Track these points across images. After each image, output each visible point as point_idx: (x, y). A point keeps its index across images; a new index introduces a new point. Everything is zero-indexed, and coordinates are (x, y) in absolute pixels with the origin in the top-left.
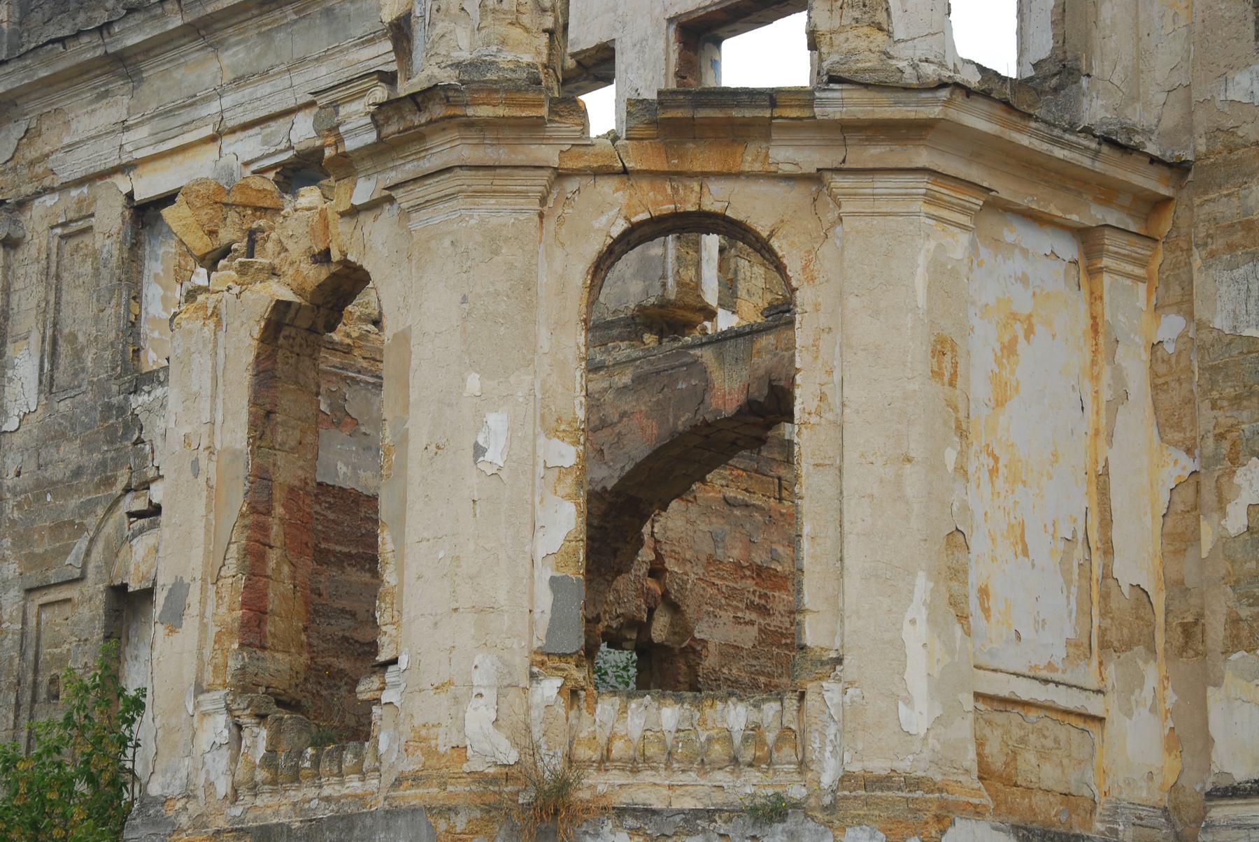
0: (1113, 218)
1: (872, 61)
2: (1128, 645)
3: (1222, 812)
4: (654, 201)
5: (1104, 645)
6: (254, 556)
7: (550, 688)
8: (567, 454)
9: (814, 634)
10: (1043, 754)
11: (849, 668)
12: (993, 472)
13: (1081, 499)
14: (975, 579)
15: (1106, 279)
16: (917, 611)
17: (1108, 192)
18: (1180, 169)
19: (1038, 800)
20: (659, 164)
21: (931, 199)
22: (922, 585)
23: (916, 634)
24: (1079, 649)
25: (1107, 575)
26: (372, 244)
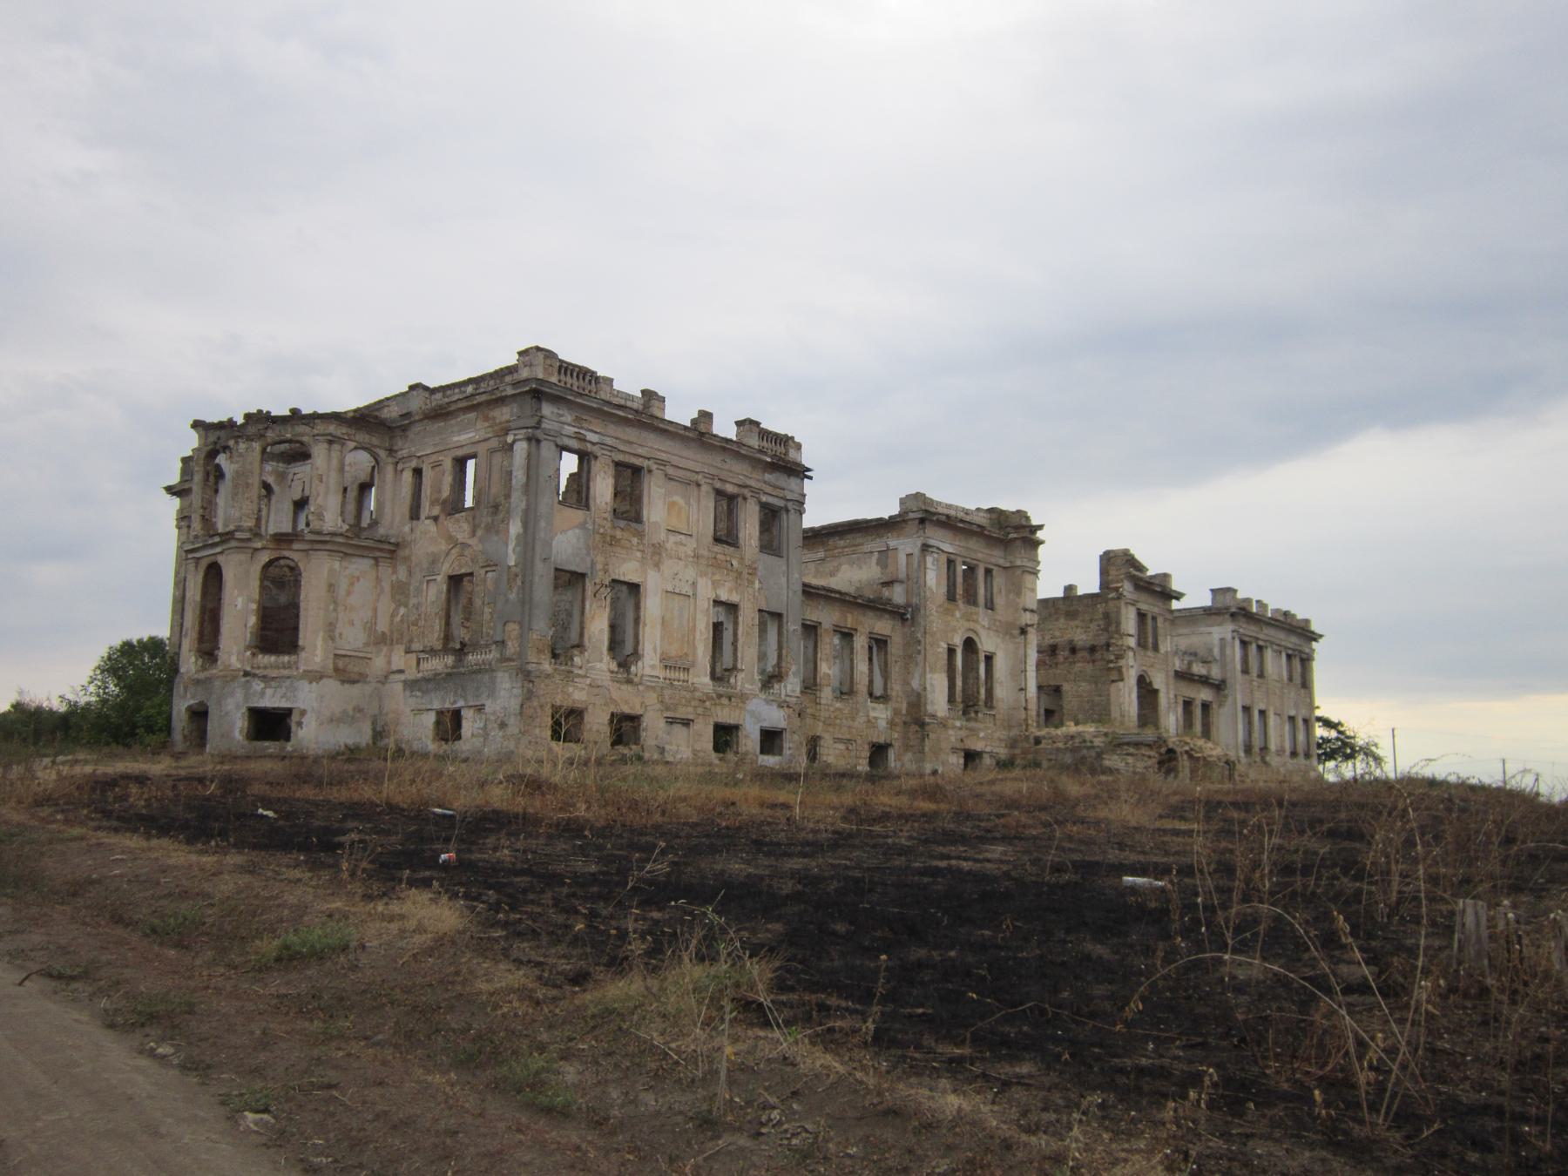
4: (275, 555)
6: (202, 624)
8: (254, 606)
9: (301, 643)
13: (370, 614)
14: (337, 631)
17: (381, 550)
18: (397, 545)
23: (319, 643)
24: (367, 644)
26: (221, 560)
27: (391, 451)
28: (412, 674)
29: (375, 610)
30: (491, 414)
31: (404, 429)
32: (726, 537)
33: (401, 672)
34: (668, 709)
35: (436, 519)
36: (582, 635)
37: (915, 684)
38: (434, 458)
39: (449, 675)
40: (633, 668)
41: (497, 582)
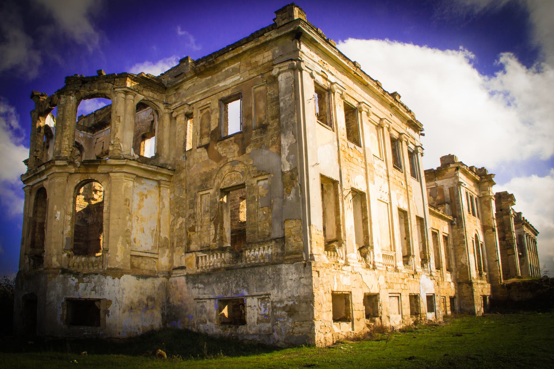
0: (164, 179)
1: (117, 155)
2: (163, 247)
3: (175, 272)
4: (85, 177)
5: (159, 247)
7: (65, 255)
10: (146, 264)
11: (109, 252)
12: (138, 220)
13: (156, 224)
14: (132, 237)
15: (162, 188)
16: (120, 242)
17: (163, 175)
19: (144, 271)
20: (85, 172)
21: (125, 176)
22: (121, 238)
23: (119, 246)
24: (154, 247)
25: (159, 236)
26: (46, 184)
27: (167, 105)
28: (192, 269)
29: (159, 220)
30: (253, 60)
31: (177, 87)
32: (397, 164)
33: (183, 268)
34: (390, 287)
35: (206, 147)
36: (338, 231)
37: (463, 261)
38: (203, 103)
39: (227, 269)
40: (368, 257)
41: (270, 188)
